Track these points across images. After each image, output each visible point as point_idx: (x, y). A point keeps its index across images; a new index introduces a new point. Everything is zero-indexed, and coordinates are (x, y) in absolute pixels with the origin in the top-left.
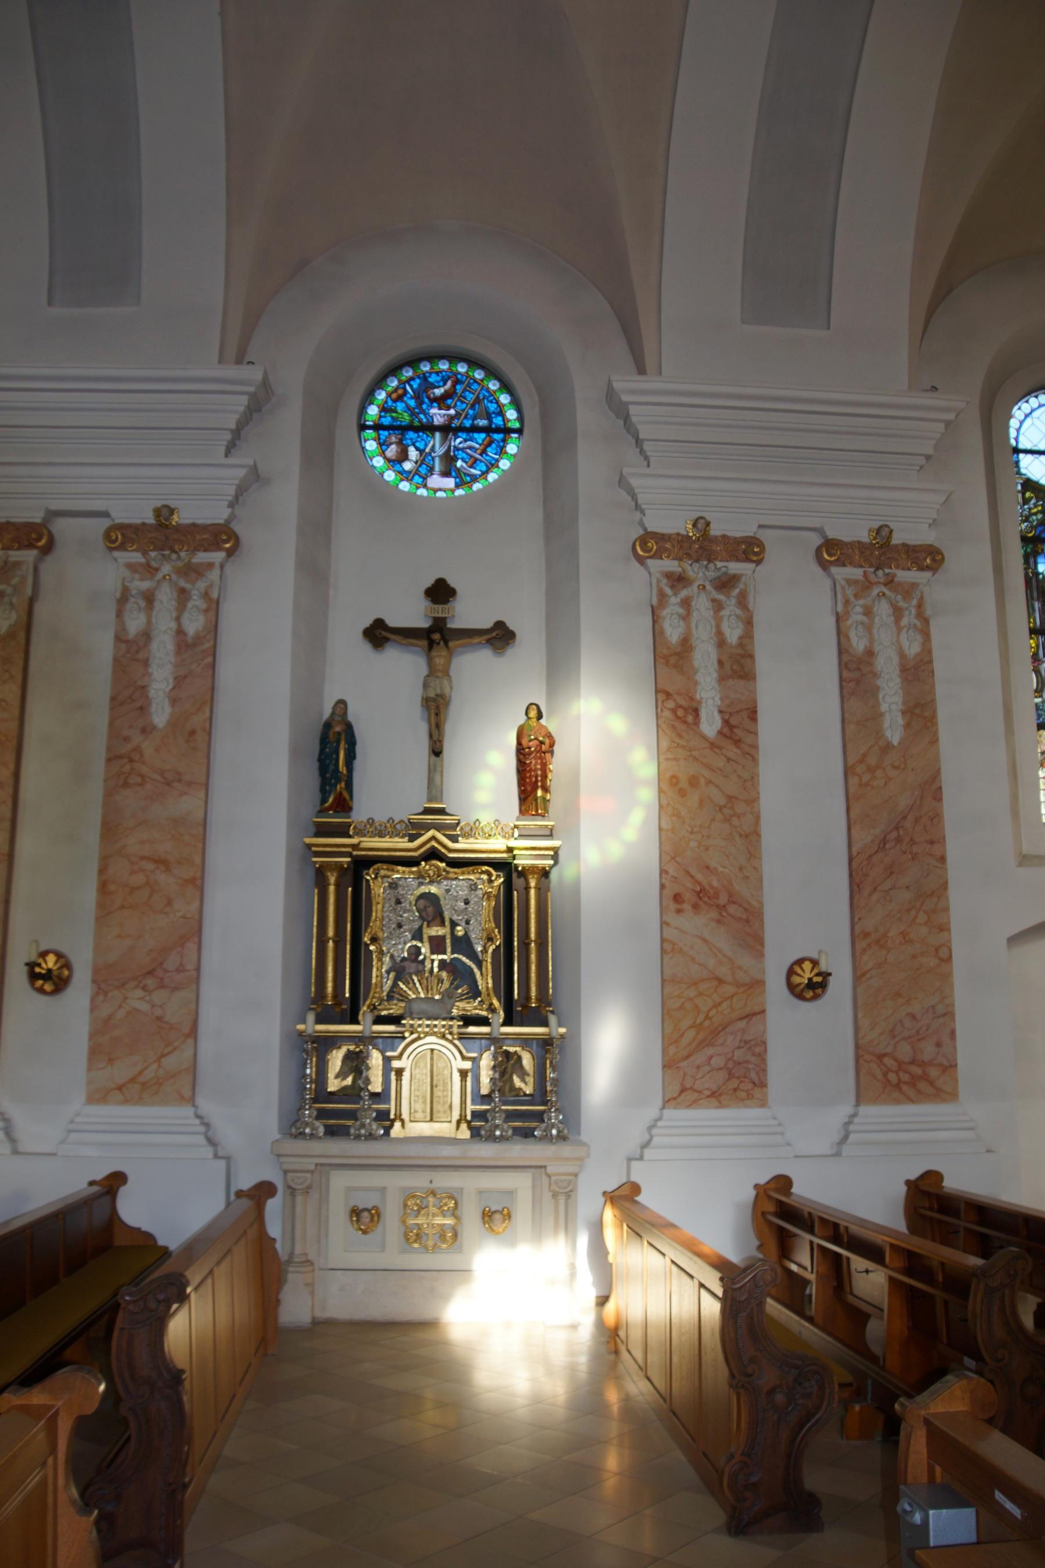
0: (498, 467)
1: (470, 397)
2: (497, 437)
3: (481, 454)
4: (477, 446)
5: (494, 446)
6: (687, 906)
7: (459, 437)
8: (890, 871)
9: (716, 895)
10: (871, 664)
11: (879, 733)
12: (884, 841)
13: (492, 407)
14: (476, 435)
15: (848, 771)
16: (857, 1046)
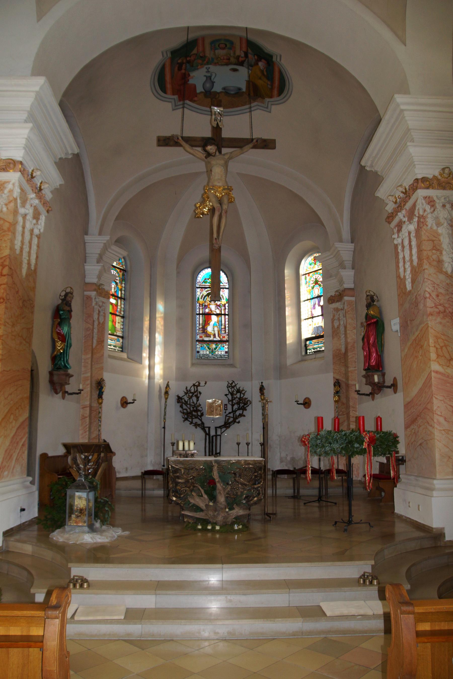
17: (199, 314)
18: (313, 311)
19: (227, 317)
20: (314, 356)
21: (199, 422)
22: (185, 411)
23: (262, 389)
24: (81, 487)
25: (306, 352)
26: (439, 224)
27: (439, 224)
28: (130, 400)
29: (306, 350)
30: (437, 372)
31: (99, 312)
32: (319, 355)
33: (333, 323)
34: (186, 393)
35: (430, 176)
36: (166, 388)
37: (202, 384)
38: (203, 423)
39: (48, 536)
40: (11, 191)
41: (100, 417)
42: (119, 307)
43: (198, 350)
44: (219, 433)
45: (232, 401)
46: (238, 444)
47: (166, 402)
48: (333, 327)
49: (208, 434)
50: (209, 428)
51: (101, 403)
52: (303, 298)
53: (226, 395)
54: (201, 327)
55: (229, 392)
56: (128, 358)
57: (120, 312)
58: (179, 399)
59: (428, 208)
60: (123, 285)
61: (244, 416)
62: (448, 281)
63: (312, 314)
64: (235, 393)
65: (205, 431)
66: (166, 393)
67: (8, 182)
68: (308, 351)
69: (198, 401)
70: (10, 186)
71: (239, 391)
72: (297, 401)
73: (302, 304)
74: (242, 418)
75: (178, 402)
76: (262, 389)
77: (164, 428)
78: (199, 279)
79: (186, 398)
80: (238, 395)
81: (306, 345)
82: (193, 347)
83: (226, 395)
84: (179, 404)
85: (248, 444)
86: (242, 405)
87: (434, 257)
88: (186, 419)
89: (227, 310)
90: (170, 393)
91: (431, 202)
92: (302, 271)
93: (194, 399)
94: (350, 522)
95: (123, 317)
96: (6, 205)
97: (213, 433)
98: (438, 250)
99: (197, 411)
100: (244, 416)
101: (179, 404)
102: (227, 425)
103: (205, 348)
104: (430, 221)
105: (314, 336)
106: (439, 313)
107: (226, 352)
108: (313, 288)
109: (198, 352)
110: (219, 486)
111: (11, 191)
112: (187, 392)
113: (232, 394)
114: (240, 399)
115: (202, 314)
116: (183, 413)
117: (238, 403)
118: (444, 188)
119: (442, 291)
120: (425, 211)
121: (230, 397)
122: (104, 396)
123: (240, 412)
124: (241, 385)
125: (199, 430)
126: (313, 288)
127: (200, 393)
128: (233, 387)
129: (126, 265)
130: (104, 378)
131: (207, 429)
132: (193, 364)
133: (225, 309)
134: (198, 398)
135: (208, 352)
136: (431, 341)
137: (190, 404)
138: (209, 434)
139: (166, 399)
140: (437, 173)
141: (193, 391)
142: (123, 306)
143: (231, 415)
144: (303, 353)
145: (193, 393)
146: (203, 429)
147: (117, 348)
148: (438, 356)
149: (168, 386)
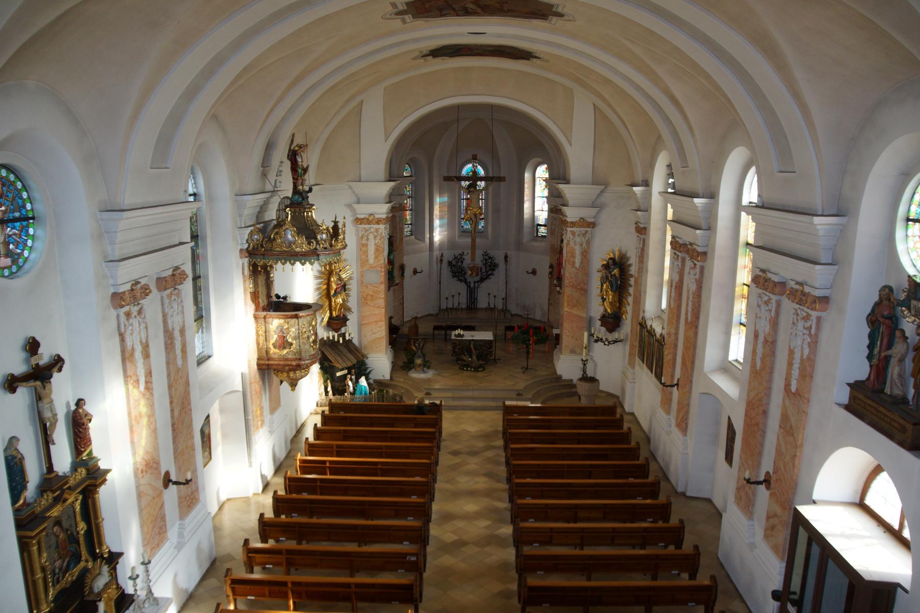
0: (27, 246)
1: (10, 195)
2: (25, 223)
3: (19, 238)
4: (17, 232)
5: (24, 230)
6: (144, 473)
7: (9, 227)
8: (183, 423)
9: (150, 464)
10: (173, 333)
11: (176, 364)
12: (180, 411)
13: (20, 201)
14: (16, 224)
15: (170, 387)
16: (179, 498)
17: (463, 199)
18: (543, 206)
19: (483, 201)
20: (541, 239)
21: (463, 278)
22: (454, 271)
23: (506, 257)
24: (419, 357)
25: (537, 234)
26: (575, 245)
27: (575, 245)
28: (419, 270)
29: (537, 232)
30: (566, 311)
31: (400, 221)
32: (544, 239)
33: (551, 225)
34: (454, 259)
35: (574, 221)
36: (441, 256)
37: (465, 253)
38: (466, 279)
39: (407, 375)
40: (381, 233)
41: (403, 288)
42: (408, 204)
43: (462, 225)
44: (476, 285)
45: (486, 264)
46: (489, 294)
47: (441, 266)
48: (551, 228)
49: (469, 286)
50: (470, 283)
51: (403, 279)
52: (536, 195)
53: (482, 261)
54: (464, 208)
55: (484, 259)
56: (416, 238)
57: (409, 208)
58: (450, 263)
59: (571, 236)
60: (410, 187)
61: (493, 275)
62: (576, 271)
63: (542, 208)
64: (488, 258)
65: (467, 285)
66: (441, 260)
67: (380, 229)
68: (539, 233)
69: (462, 264)
70: (381, 231)
71: (490, 258)
72: (527, 272)
73: (537, 200)
74: (492, 276)
75: (449, 265)
76: (506, 257)
77: (440, 283)
78: (463, 172)
79: (454, 263)
80: (490, 260)
81: (537, 230)
82: (460, 223)
83: (482, 261)
84: (450, 267)
85: (495, 296)
86: (492, 267)
87: (572, 260)
88: (454, 277)
89: (483, 196)
90: (443, 260)
91: (573, 233)
92: (537, 175)
93: (460, 263)
94: (527, 369)
95: (411, 210)
96: (380, 240)
97: (472, 285)
98: (573, 257)
99: (462, 270)
100: (493, 275)
101: (450, 267)
102: (482, 280)
103: (467, 224)
104: (572, 244)
105: (543, 224)
106: (570, 286)
107: (482, 227)
108: (544, 189)
109: (463, 227)
110: (474, 351)
111: (381, 233)
112: (456, 258)
113: (486, 260)
114: (491, 262)
115: (465, 199)
116: (452, 272)
117: (490, 266)
118: (581, 227)
119: (573, 276)
120: (570, 238)
121: (484, 262)
122: (405, 274)
123: (491, 272)
124: (492, 253)
125: (463, 283)
126: (544, 189)
127: (464, 259)
128: (486, 255)
129: (411, 172)
130: (404, 263)
131: (468, 283)
132: (459, 236)
133: (482, 195)
134: (462, 262)
135: (469, 227)
136: (566, 298)
137: (457, 267)
138: (470, 287)
139: (441, 263)
140: (577, 219)
141: (459, 258)
142: (410, 202)
143: (485, 274)
144: (535, 235)
145: (459, 260)
146: (466, 282)
147: (408, 233)
148: (568, 305)
149: (442, 255)
